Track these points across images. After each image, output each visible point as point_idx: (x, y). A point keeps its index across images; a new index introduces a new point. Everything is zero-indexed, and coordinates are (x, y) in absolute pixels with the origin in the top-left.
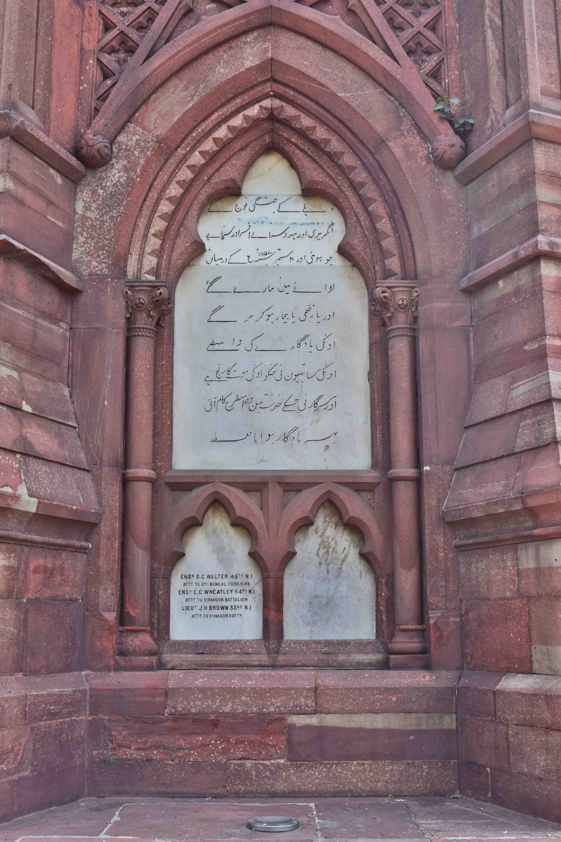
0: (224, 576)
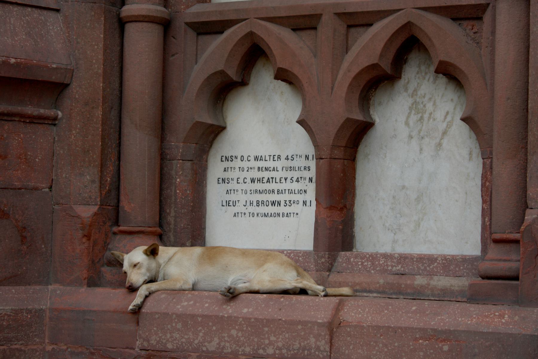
0: (276, 158)
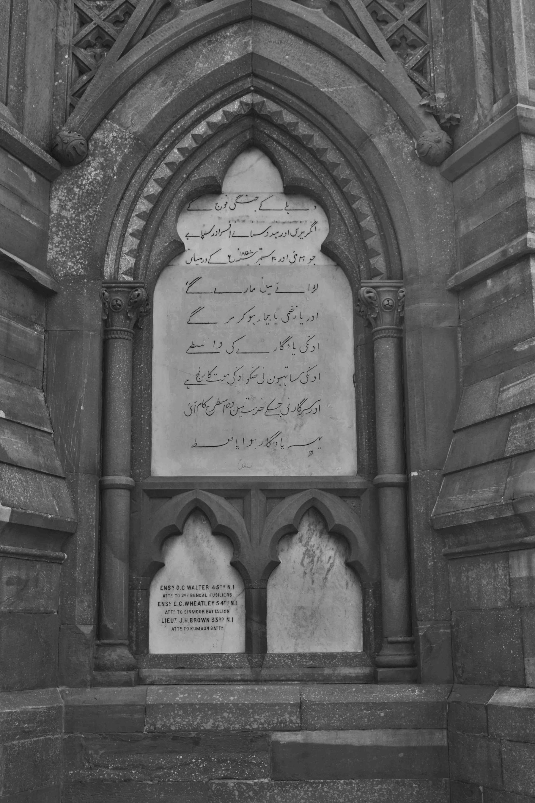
0: (205, 587)
